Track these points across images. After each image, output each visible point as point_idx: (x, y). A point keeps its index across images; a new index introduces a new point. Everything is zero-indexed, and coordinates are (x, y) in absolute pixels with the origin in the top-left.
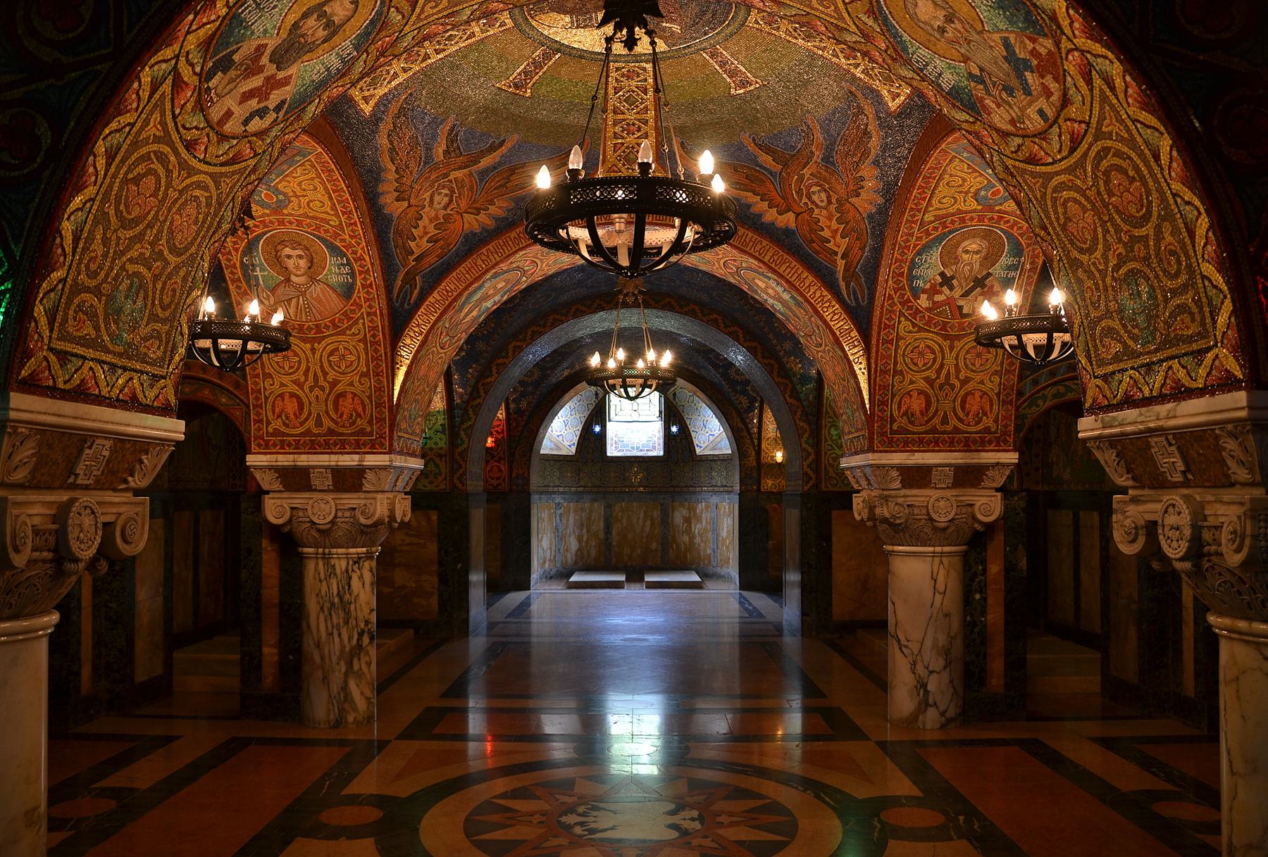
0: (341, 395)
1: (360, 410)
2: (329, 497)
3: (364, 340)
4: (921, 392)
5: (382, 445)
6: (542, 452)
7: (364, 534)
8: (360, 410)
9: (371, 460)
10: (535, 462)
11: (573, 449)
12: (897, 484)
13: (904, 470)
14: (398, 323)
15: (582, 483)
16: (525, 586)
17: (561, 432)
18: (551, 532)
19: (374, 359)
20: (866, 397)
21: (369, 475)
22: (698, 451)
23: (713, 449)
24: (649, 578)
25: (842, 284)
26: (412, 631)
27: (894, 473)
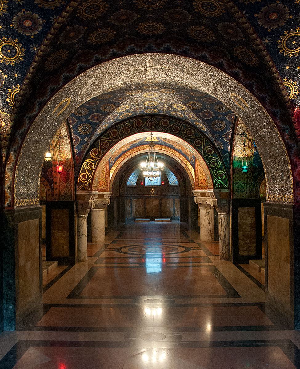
0: (100, 181)
1: (104, 184)
2: (98, 199)
3: (105, 171)
4: (204, 179)
5: (108, 190)
6: (127, 185)
7: (103, 206)
8: (104, 184)
9: (104, 193)
11: (135, 184)
12: (200, 196)
13: (201, 193)
14: (110, 168)
15: (138, 193)
16: (124, 221)
19: (106, 175)
20: (194, 179)
21: (105, 195)
22: (170, 184)
23: (174, 183)
25: (190, 160)
27: (199, 194)
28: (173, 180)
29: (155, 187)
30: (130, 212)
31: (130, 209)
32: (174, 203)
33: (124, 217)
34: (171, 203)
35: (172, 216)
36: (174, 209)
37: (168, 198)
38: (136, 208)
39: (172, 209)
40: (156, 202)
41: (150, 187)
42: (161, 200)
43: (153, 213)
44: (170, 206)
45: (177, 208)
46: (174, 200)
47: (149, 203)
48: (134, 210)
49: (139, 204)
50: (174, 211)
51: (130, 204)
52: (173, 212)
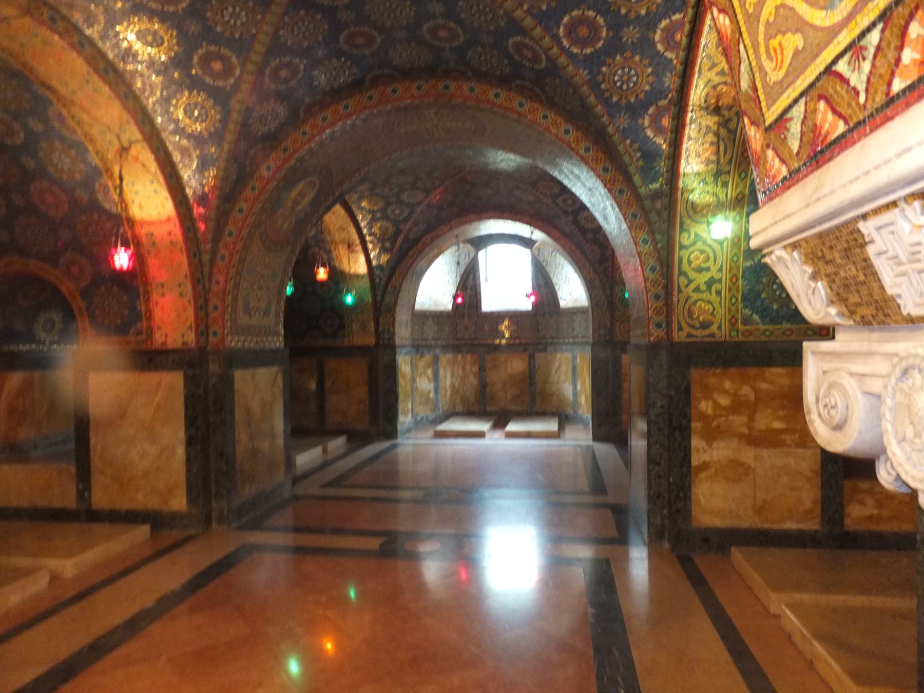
10: (402, 316)
16: (391, 433)
17: (435, 288)
18: (422, 381)
24: (512, 427)
26: (144, 531)
28: (572, 290)
29: (515, 317)
30: (432, 395)
31: (431, 386)
32: (574, 367)
33: (392, 418)
34: (564, 368)
35: (569, 411)
36: (575, 387)
37: (556, 351)
38: (453, 385)
39: (567, 389)
40: (517, 365)
41: (498, 317)
42: (532, 357)
43: (509, 397)
44: (562, 378)
45: (583, 384)
46: (574, 358)
47: (495, 366)
48: (446, 391)
49: (464, 369)
50: (575, 394)
51: (430, 371)
52: (571, 398)
